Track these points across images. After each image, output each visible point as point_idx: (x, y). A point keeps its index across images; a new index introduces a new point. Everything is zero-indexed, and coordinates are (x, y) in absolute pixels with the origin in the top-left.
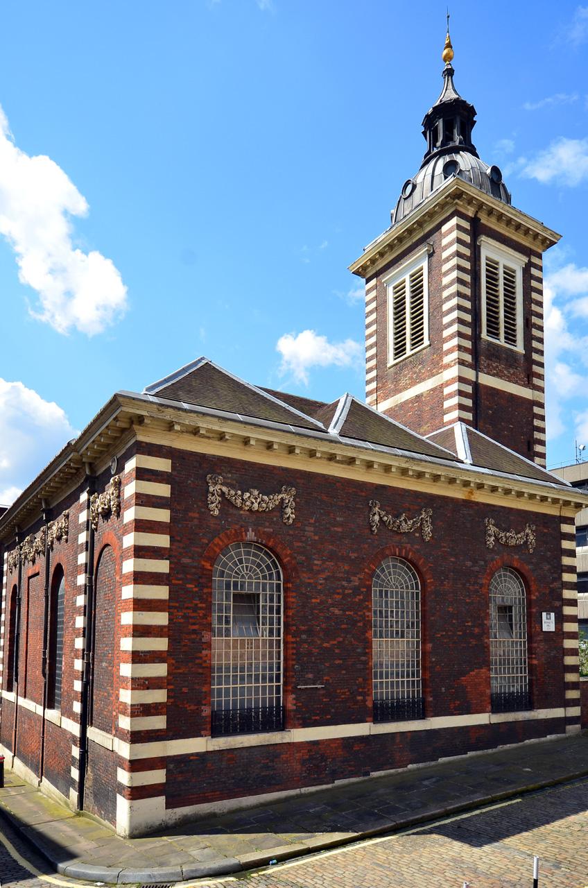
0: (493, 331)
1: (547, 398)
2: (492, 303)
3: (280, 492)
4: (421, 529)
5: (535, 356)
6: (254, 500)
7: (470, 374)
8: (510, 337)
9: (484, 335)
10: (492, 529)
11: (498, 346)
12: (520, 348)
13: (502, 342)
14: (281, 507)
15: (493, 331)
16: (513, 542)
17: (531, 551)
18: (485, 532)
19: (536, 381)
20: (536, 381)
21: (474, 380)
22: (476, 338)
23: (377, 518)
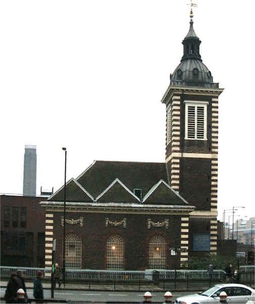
0: (191, 134)
1: (219, 156)
2: (191, 122)
3: (79, 219)
4: (122, 225)
6: (72, 222)
7: (178, 155)
8: (200, 134)
9: (186, 138)
10: (149, 222)
12: (205, 138)
13: (196, 138)
14: (79, 223)
15: (191, 134)
16: (159, 226)
17: (167, 228)
18: (147, 225)
19: (213, 150)
20: (213, 150)
22: (182, 140)
23: (107, 223)
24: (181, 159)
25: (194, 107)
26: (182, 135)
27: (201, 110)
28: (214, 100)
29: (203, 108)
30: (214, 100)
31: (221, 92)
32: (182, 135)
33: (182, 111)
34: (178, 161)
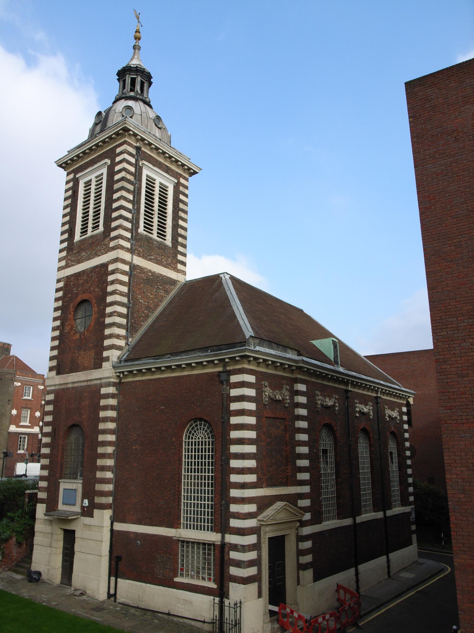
5: (180, 249)
7: (127, 256)
9: (141, 230)
11: (151, 239)
12: (168, 241)
13: (154, 236)
20: (180, 267)
21: (130, 261)
24: (133, 267)
25: (155, 180)
26: (135, 222)
27: (163, 189)
28: (182, 181)
29: (167, 187)
30: (182, 181)
31: (195, 173)
32: (135, 222)
33: (138, 174)
34: (126, 268)
